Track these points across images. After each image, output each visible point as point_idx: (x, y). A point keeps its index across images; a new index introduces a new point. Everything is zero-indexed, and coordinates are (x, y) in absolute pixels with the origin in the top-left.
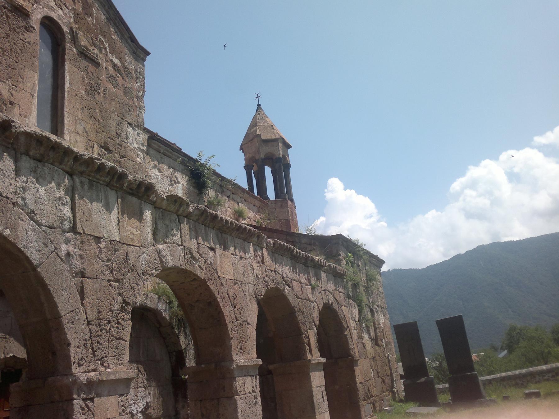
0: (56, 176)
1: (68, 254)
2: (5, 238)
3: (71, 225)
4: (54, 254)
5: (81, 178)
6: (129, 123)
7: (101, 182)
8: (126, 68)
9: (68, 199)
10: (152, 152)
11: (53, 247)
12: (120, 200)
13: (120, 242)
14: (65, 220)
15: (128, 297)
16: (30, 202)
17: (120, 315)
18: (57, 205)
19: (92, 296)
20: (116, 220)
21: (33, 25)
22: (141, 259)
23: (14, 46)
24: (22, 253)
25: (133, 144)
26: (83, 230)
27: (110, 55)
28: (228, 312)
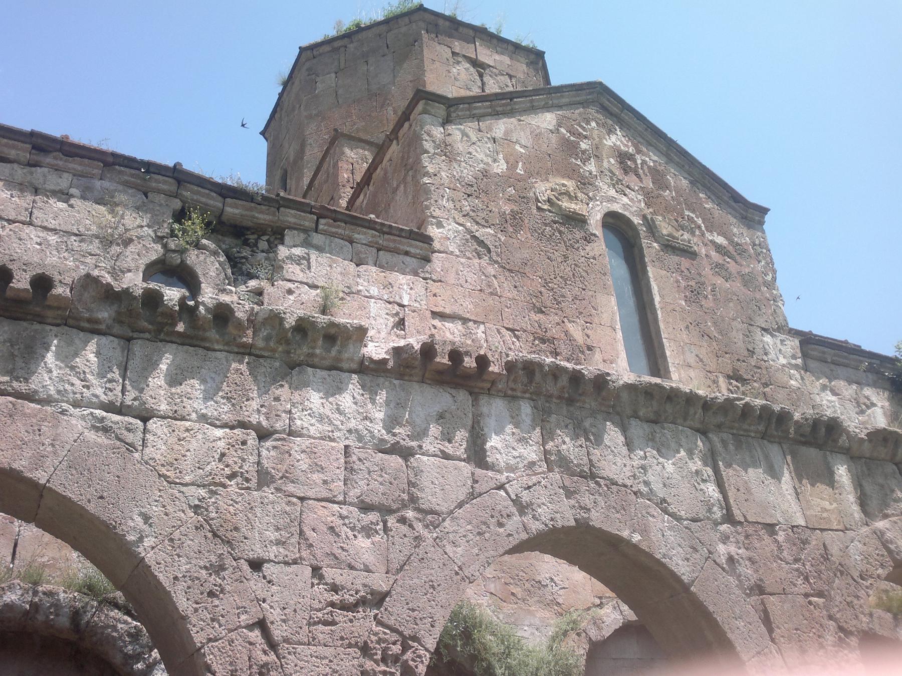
0: (683, 440)
1: (731, 559)
2: (635, 546)
3: (724, 511)
4: (710, 562)
5: (721, 434)
6: (764, 329)
7: (753, 434)
8: (738, 244)
9: (710, 471)
10: (812, 364)
11: (706, 551)
12: (789, 458)
13: (807, 527)
14: (713, 505)
15: (846, 622)
16: (657, 487)
18: (696, 484)
19: (786, 625)
20: (792, 491)
21: (594, 232)
22: (852, 551)
23: (577, 269)
24: (664, 565)
25: (778, 360)
26: (745, 517)
27: (707, 235)
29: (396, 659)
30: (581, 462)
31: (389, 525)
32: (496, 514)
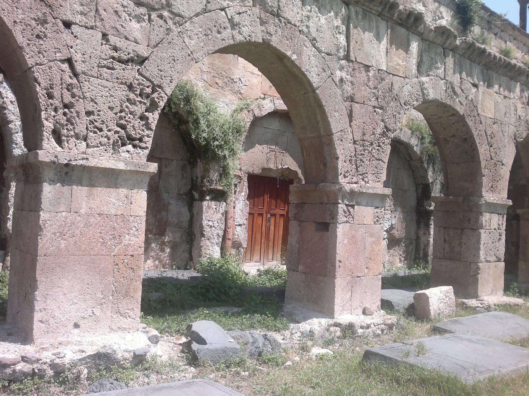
0: (335, 5)
1: (341, 80)
2: (293, 62)
3: (346, 53)
4: (330, 79)
5: (356, 8)
7: (374, 12)
9: (344, 28)
11: (330, 73)
12: (389, 31)
13: (386, 72)
14: (341, 48)
15: (389, 124)
16: (313, 30)
17: (381, 139)
18: (335, 34)
19: (359, 120)
20: (385, 50)
22: (405, 89)
24: (305, 76)
26: (356, 58)
28: (483, 150)
29: (148, 96)
30: (273, 5)
31: (152, 17)
32: (217, 25)
